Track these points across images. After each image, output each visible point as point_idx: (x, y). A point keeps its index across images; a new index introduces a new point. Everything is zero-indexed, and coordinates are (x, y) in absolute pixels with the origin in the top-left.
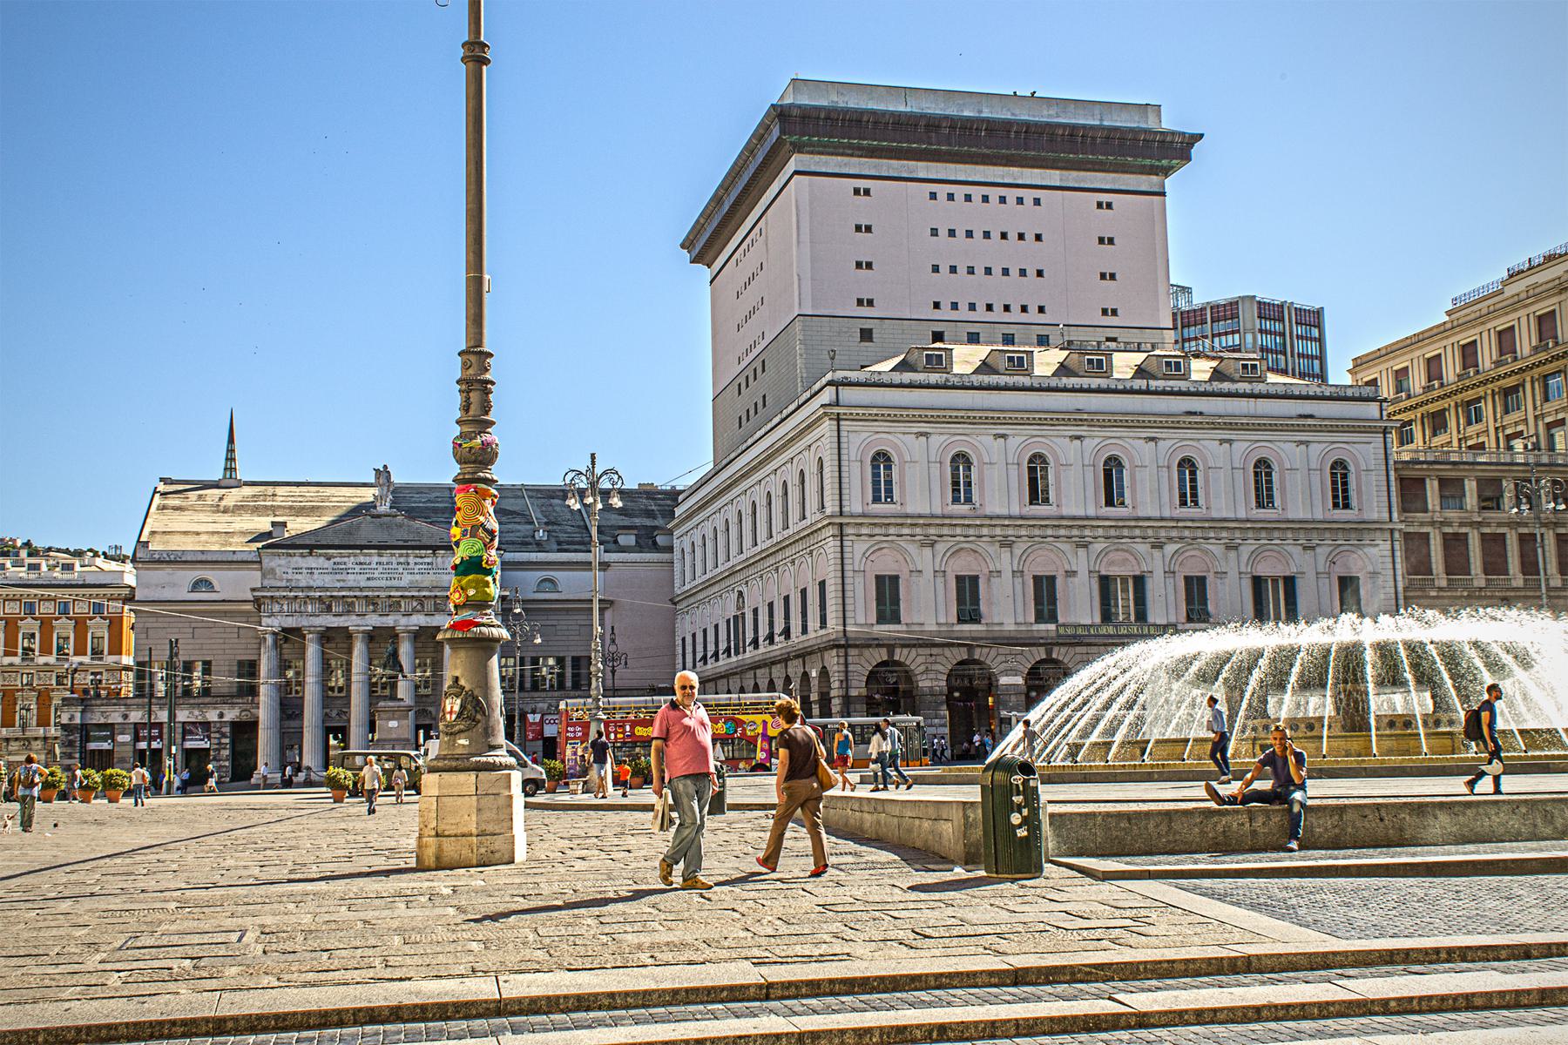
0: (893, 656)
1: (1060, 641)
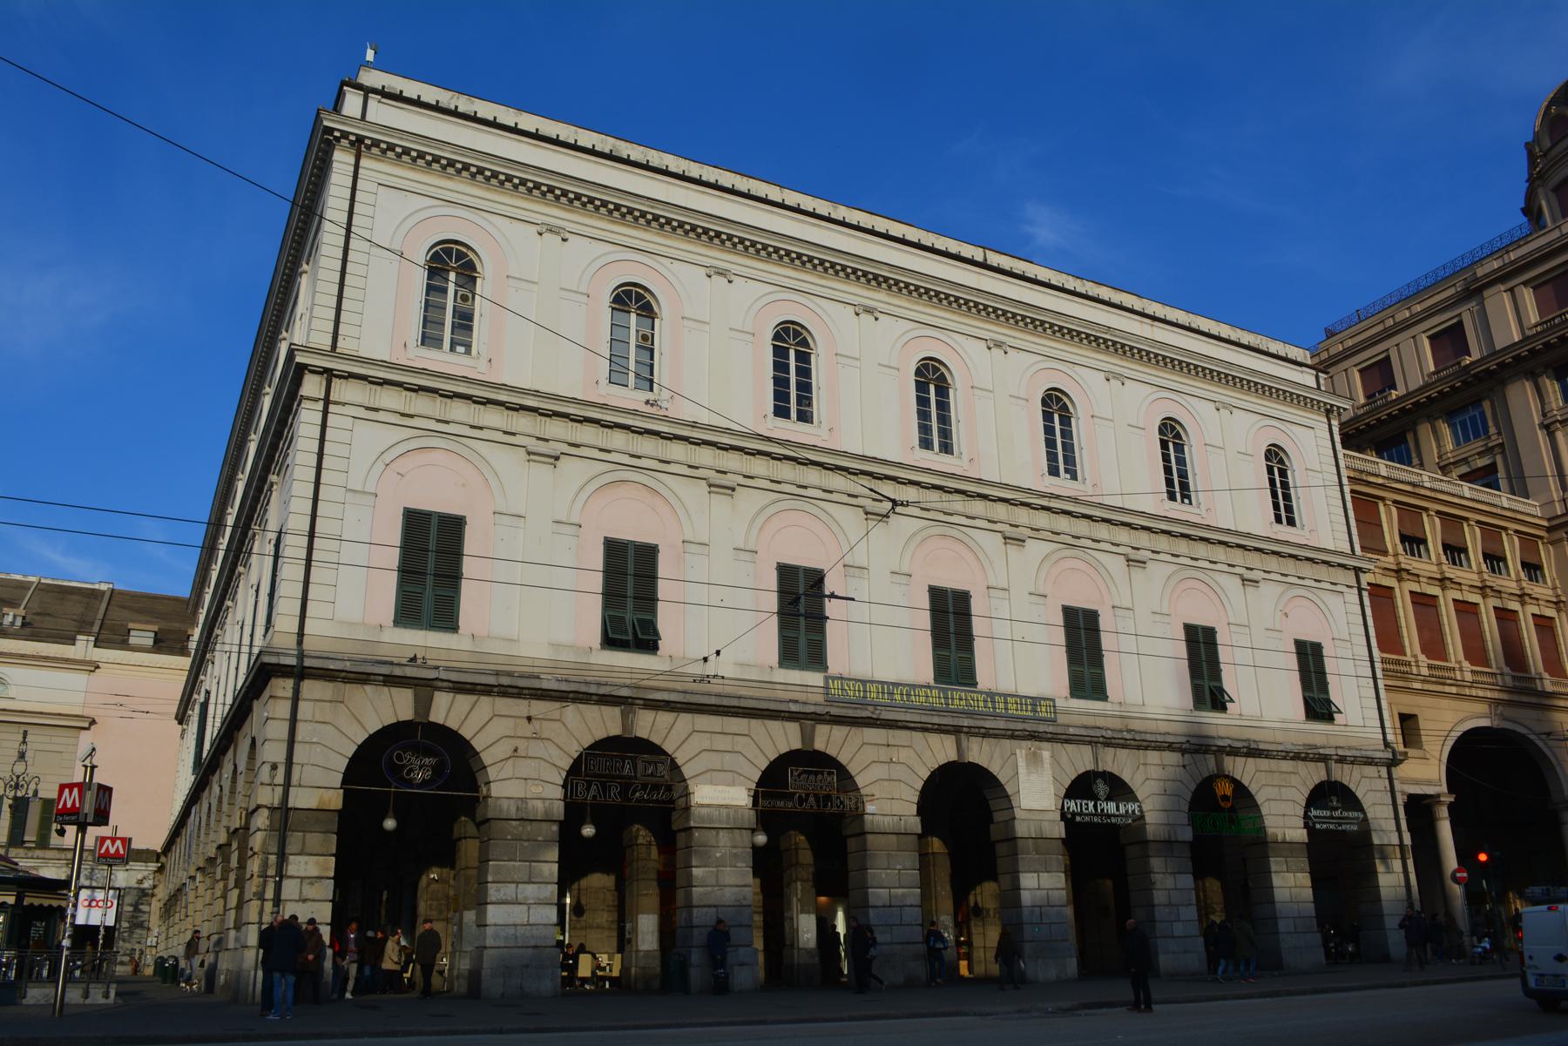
0: (427, 714)
1: (835, 711)
